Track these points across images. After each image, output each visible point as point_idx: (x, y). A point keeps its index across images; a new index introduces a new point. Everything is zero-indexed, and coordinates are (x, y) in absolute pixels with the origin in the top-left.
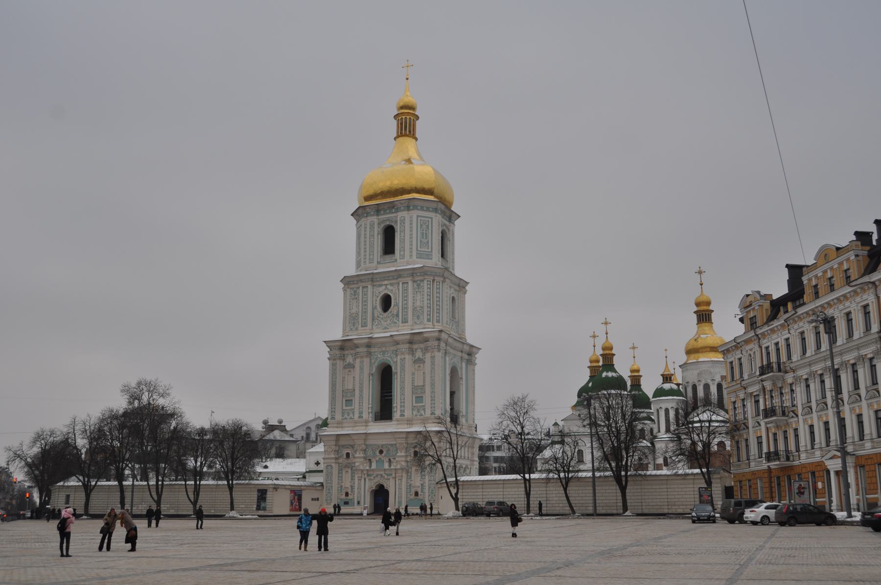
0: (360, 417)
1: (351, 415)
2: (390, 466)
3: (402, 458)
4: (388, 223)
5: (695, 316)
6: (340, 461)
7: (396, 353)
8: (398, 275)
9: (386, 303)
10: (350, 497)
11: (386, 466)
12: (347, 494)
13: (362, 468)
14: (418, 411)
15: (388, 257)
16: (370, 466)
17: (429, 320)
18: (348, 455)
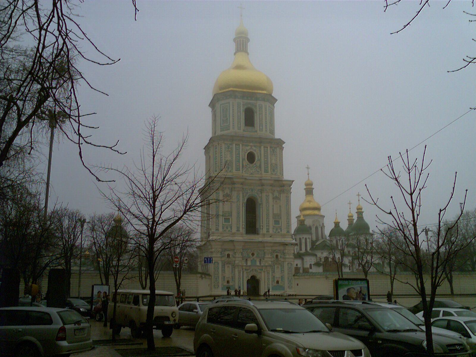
0: (238, 230)
1: (229, 229)
2: (260, 264)
3: (269, 259)
4: (249, 106)
5: (304, 191)
6: (223, 259)
8: (261, 141)
9: (251, 158)
10: (231, 284)
11: (258, 264)
12: (228, 282)
13: (240, 264)
14: (277, 230)
15: (250, 128)
16: (247, 264)
18: (228, 256)
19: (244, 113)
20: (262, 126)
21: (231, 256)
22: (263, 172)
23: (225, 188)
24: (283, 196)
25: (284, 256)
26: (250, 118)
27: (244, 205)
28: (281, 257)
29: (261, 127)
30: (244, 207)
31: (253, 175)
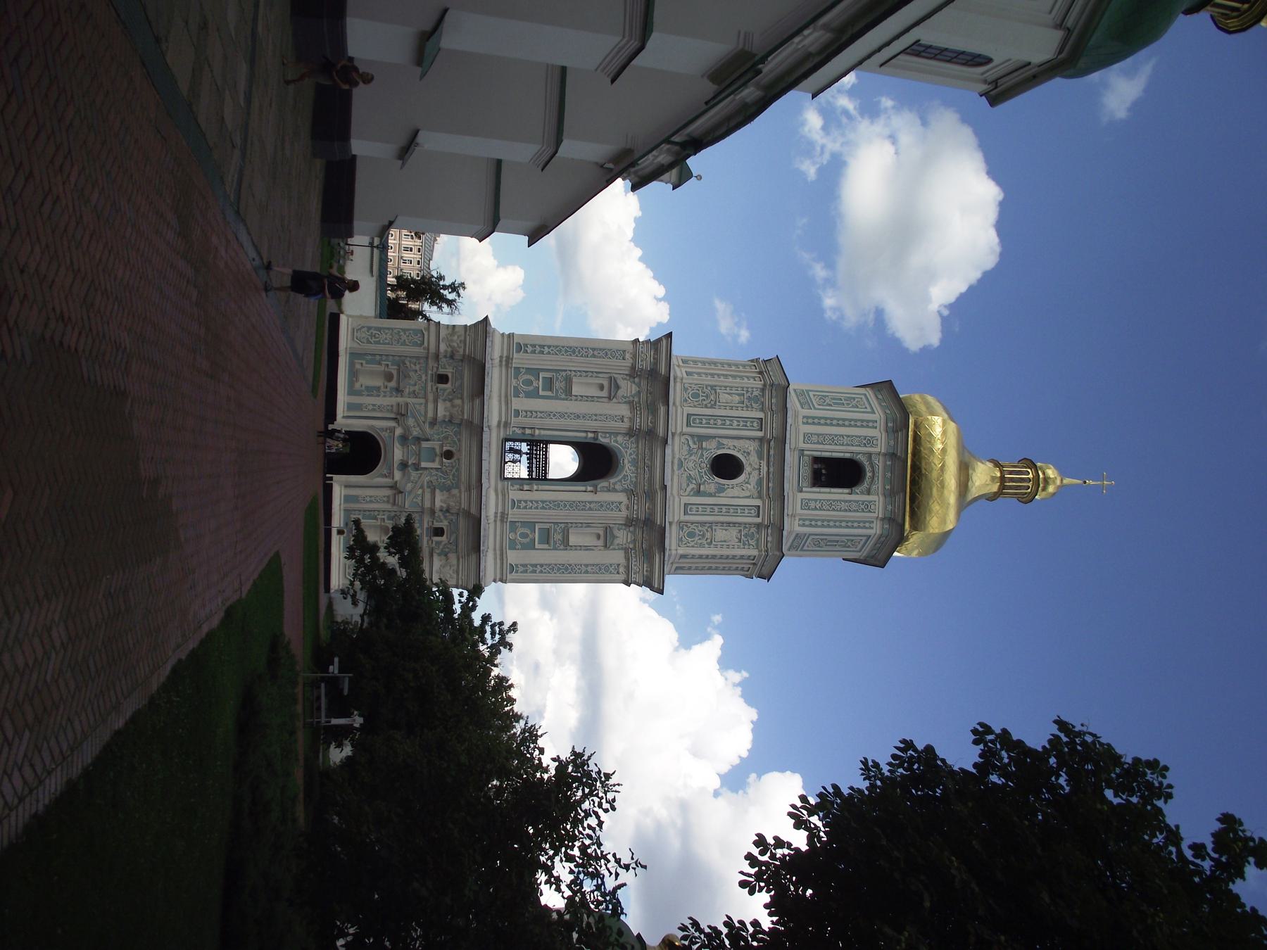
4: (869, 474)
7: (630, 493)
9: (726, 467)
15: (807, 471)
17: (683, 556)
19: (848, 455)
20: (816, 509)
21: (441, 386)
22: (685, 500)
23: (639, 385)
24: (617, 557)
25: (439, 555)
26: (838, 472)
27: (590, 435)
28: (438, 543)
29: (812, 505)
30: (583, 435)
31: (676, 467)
